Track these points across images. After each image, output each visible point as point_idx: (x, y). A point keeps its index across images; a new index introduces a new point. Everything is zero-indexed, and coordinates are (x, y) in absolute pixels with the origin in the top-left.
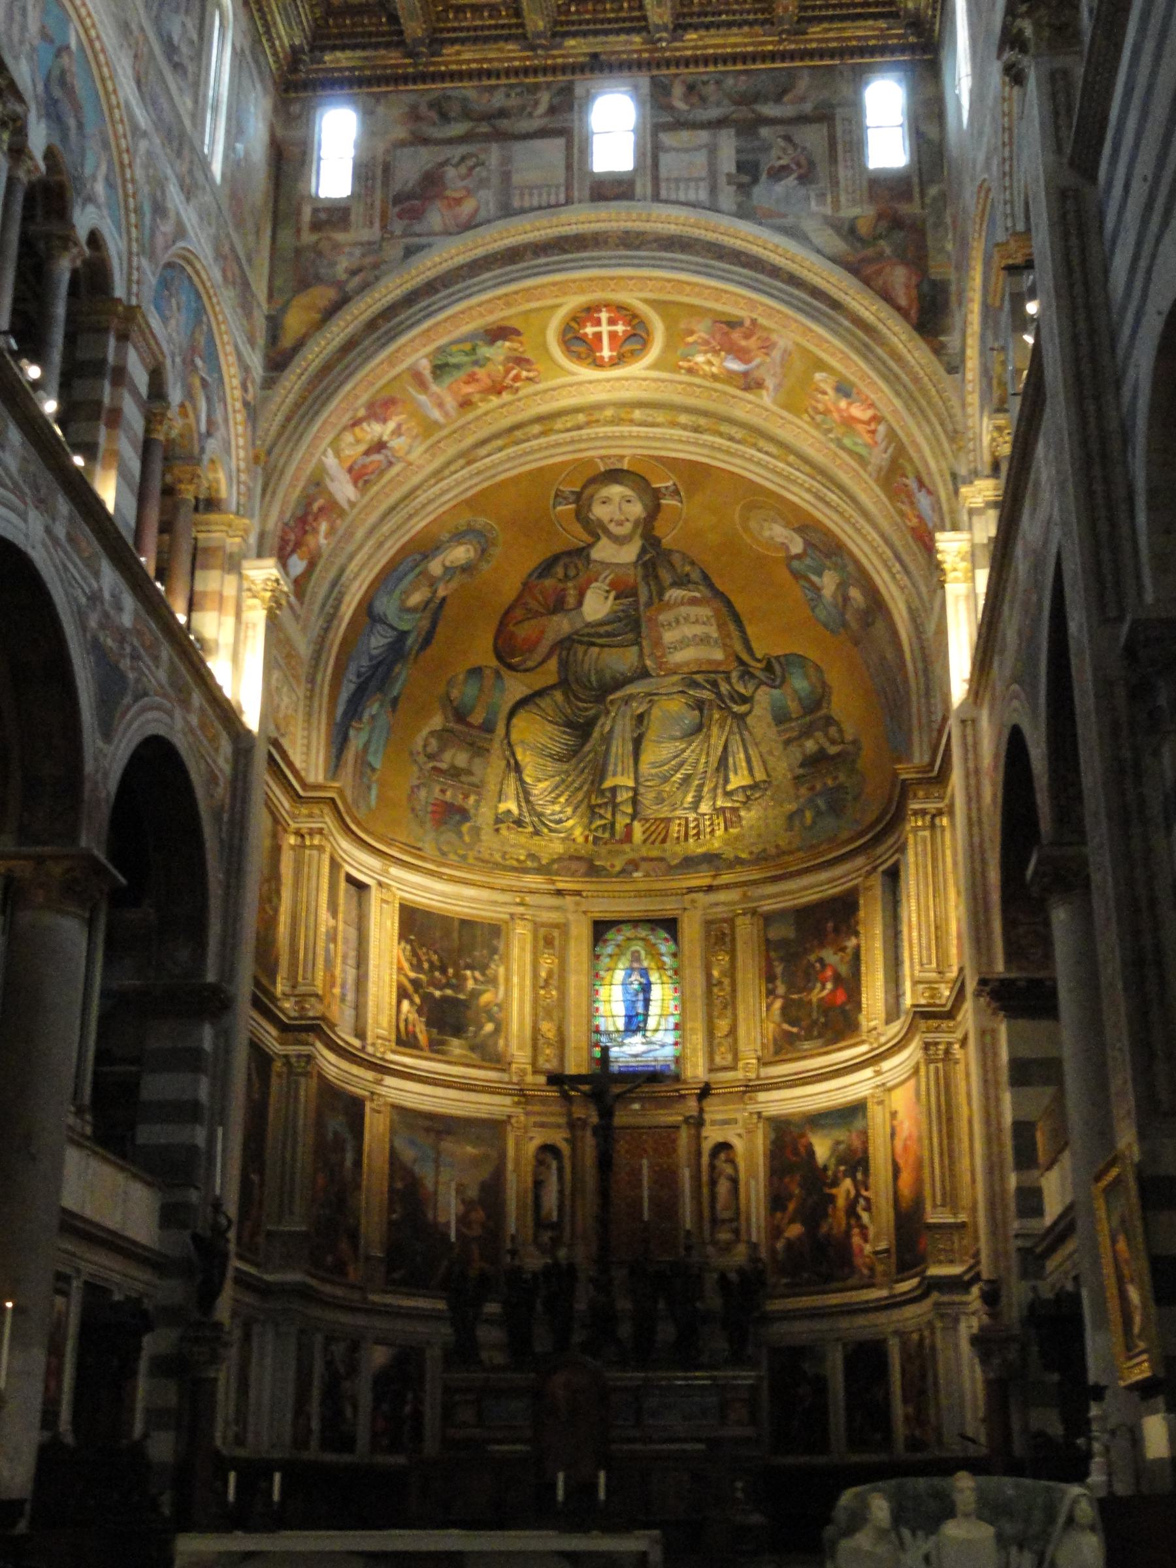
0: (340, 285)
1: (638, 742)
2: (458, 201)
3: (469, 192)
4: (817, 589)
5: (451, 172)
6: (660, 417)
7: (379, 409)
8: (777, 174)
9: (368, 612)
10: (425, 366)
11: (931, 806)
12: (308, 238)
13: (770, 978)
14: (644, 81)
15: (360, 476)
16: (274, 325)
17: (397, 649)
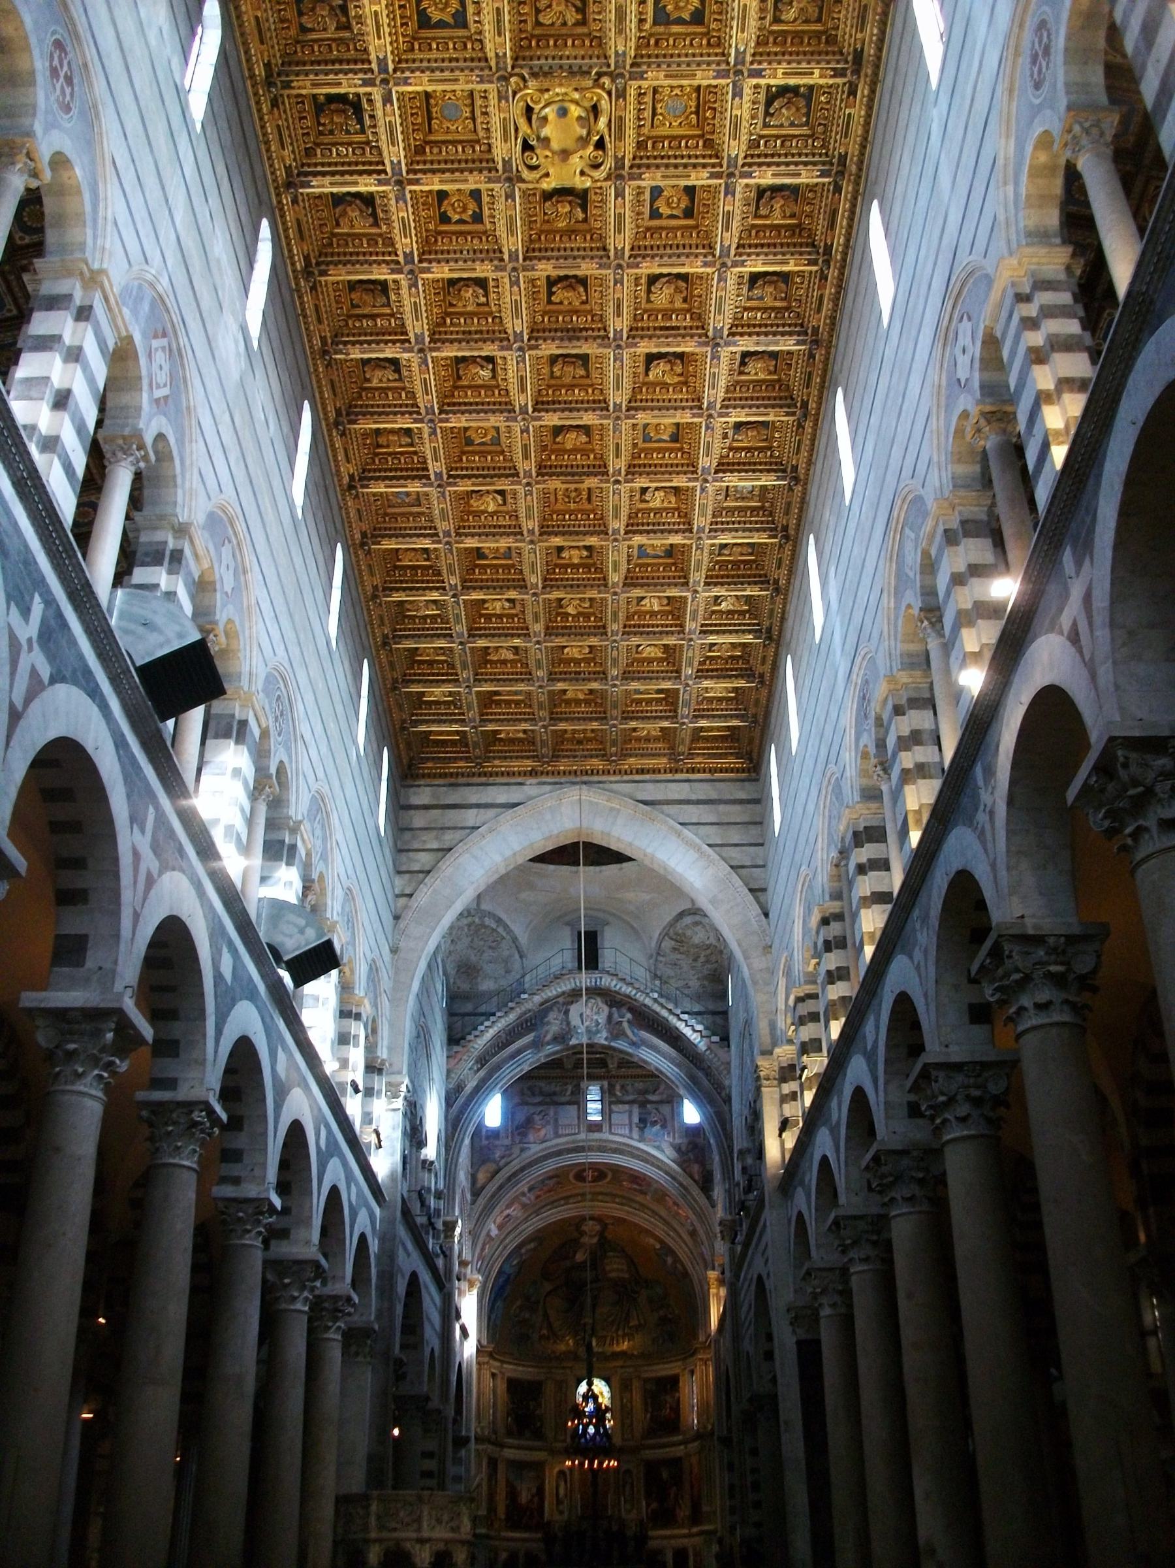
0: (497, 1163)
1: (594, 1306)
2: (539, 1130)
3: (543, 1126)
4: (665, 1262)
5: (537, 1118)
6: (608, 1198)
7: (508, 1207)
8: (654, 1123)
9: (500, 1272)
10: (526, 1190)
11: (705, 1357)
12: (485, 1142)
13: (646, 1404)
14: (605, 1083)
15: (500, 1227)
16: (474, 1178)
17: (507, 1281)
